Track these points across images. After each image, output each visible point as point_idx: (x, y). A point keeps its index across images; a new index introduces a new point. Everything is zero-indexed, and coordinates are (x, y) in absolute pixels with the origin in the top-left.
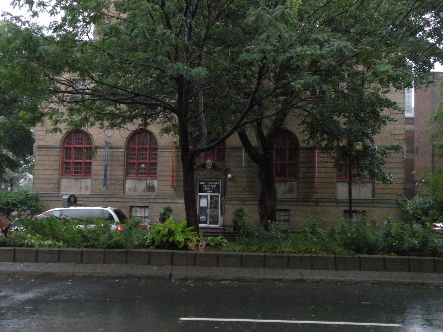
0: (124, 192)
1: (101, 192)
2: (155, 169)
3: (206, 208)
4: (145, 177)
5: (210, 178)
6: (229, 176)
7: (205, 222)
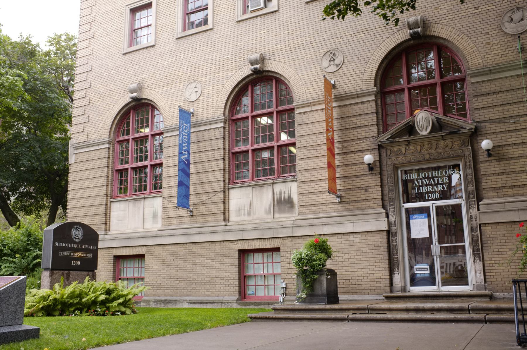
0: (226, 219)
1: (179, 224)
4: (273, 179)
5: (430, 161)
6: (486, 144)
7: (431, 281)
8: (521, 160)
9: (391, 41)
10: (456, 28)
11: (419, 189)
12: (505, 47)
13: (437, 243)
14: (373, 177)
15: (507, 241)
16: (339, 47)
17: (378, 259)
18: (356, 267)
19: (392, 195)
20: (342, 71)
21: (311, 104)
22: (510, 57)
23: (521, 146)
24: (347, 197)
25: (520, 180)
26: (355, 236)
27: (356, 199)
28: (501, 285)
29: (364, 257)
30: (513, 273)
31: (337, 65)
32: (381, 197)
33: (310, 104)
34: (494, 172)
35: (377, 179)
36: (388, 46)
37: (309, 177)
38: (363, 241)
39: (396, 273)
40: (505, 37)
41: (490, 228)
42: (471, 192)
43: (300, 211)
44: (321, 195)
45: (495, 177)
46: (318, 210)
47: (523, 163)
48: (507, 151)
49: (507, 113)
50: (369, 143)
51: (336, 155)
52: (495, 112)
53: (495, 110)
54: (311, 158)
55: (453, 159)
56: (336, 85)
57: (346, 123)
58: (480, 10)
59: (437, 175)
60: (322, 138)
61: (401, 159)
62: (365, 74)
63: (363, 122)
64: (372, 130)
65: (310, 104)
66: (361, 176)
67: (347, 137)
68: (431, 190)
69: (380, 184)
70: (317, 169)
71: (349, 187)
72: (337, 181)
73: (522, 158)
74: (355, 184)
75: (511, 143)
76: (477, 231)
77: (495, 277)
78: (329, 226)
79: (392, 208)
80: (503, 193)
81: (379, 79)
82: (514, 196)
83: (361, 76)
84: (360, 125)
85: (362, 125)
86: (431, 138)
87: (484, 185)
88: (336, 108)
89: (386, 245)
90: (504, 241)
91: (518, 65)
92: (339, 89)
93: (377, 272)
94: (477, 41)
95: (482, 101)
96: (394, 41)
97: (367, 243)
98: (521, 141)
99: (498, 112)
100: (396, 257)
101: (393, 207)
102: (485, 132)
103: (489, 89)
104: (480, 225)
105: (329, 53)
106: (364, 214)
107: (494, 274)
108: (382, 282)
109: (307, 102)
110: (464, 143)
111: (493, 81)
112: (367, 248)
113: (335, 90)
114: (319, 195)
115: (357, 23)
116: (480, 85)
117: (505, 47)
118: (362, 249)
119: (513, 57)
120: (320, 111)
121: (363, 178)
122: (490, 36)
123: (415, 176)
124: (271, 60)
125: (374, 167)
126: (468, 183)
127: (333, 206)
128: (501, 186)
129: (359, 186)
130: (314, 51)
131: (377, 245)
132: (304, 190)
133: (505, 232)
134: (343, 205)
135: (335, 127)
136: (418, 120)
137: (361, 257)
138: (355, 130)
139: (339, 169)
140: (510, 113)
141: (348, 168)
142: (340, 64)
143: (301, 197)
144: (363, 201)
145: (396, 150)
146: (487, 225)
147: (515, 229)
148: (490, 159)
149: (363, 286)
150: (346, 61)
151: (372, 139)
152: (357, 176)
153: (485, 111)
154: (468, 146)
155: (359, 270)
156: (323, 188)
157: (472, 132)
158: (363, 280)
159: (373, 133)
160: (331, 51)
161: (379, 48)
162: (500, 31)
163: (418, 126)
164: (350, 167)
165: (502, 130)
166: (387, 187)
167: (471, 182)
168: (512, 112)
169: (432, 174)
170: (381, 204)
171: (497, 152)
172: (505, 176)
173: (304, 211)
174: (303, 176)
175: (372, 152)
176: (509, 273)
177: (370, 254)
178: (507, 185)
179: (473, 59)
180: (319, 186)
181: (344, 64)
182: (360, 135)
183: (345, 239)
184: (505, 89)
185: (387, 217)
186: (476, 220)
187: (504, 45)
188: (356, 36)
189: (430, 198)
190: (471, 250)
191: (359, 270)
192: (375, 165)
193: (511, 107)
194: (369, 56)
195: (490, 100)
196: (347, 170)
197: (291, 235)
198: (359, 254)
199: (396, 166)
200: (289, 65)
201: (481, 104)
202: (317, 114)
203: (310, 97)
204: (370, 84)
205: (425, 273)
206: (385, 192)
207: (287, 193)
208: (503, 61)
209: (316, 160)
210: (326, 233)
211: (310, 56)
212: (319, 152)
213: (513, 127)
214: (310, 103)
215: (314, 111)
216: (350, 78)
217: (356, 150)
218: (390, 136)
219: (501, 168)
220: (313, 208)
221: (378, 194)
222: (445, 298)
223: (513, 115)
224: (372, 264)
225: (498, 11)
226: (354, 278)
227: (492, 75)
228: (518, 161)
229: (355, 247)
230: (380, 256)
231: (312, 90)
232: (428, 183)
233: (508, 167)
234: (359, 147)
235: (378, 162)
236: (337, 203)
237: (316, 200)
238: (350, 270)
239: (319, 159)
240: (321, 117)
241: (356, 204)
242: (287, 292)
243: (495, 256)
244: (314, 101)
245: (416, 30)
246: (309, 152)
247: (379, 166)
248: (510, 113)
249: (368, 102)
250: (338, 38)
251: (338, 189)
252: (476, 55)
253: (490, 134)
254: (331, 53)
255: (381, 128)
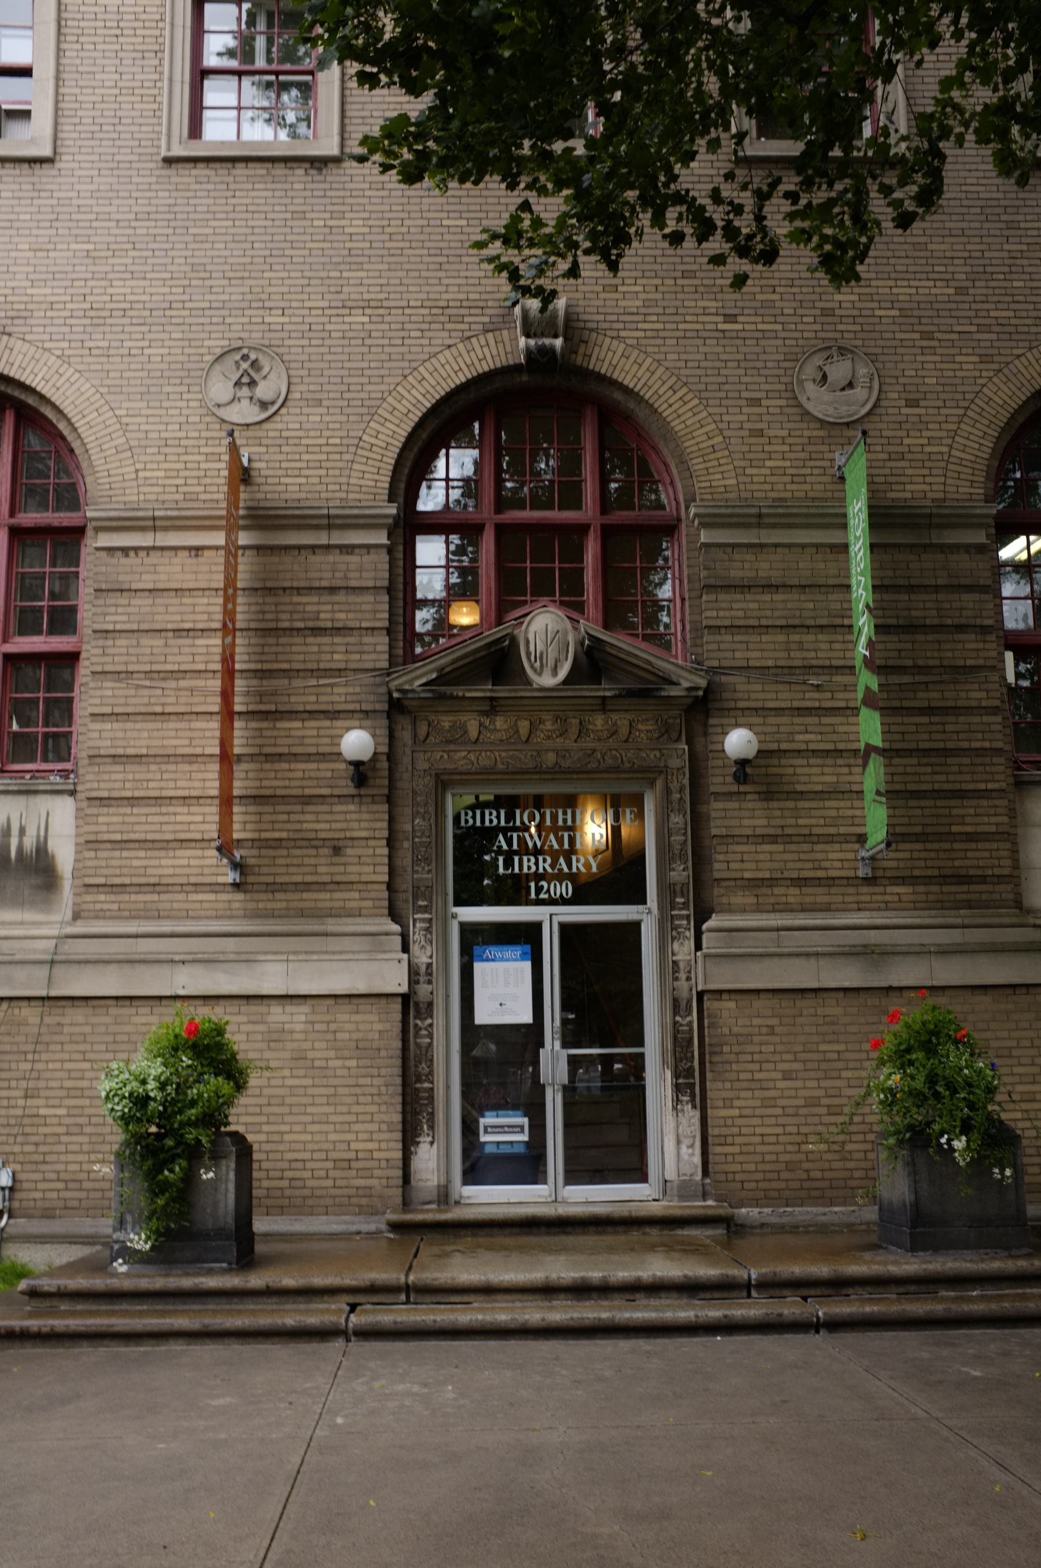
2: (64, 709)
3: (533, 1034)
8: (828, 804)
9: (460, 360)
10: (667, 364)
11: (509, 863)
12: (802, 455)
13: (557, 1045)
14: (364, 808)
15: (779, 1048)
16: (273, 342)
17: (368, 1090)
18: (287, 1119)
19: (424, 875)
20: (279, 426)
21: (153, 524)
22: (815, 487)
23: (829, 761)
24: (264, 870)
25: (824, 864)
26: (290, 1008)
27: (299, 879)
28: (753, 1185)
29: (317, 1081)
30: (790, 1148)
31: (264, 405)
32: (386, 878)
33: (151, 523)
34: (750, 832)
35: (377, 816)
36: (445, 375)
37: (127, 785)
38: (317, 1027)
39: (425, 1140)
40: (805, 425)
41: (732, 1005)
42: (678, 888)
43: (85, 907)
44: (171, 853)
45: (752, 848)
46: (154, 906)
47: (833, 813)
48: (791, 771)
49: (798, 654)
50: (358, 689)
51: (236, 717)
52: (765, 646)
53: (764, 638)
54: (139, 718)
55: (630, 775)
56: (253, 473)
57: (279, 608)
58: (739, 327)
59: (569, 823)
60: (187, 650)
61: (462, 758)
62: (360, 452)
63: (342, 616)
64: (371, 648)
65: (151, 523)
66: (321, 800)
67: (281, 657)
68: (549, 870)
69: (385, 834)
70: (159, 759)
71: (277, 835)
72: (236, 809)
73: (834, 796)
74: (298, 826)
75: (803, 747)
76: (690, 1013)
77: (738, 1158)
78: (198, 970)
79: (423, 920)
80: (772, 900)
81: (404, 478)
82: (804, 909)
83: (346, 457)
84: (329, 625)
85: (337, 625)
86: (566, 702)
87: (719, 868)
88: (247, 552)
89: (399, 1044)
90: (771, 1048)
91: (836, 515)
92: (262, 488)
93: (361, 1136)
94: (725, 418)
95: (728, 606)
96: (469, 362)
97: (330, 1036)
98: (830, 746)
99: (772, 646)
100: (426, 1085)
101: (427, 916)
102: (732, 704)
103: (753, 574)
104: (700, 995)
105: (237, 357)
106: (326, 934)
107: (737, 1149)
108: (377, 1173)
109: (140, 514)
110: (666, 730)
111: (765, 550)
112: (332, 1054)
113: (249, 488)
114: (163, 853)
115: (345, 274)
116: (726, 557)
117: (802, 455)
118: (310, 1055)
119: (822, 487)
120: (186, 553)
121: (325, 808)
122: (764, 410)
123: (498, 817)
124: (10, 335)
125: (369, 774)
126: (672, 860)
127: (211, 897)
128: (768, 876)
129: (313, 835)
130: (180, 336)
131: (367, 1045)
132: (104, 828)
133: (775, 1021)
134: (248, 896)
135: (239, 617)
136: (531, 637)
137: (308, 1082)
138: (310, 640)
139: (244, 766)
140: (805, 654)
141: (276, 766)
142: (273, 403)
143: (92, 854)
144: (322, 887)
145: (447, 725)
146: (725, 996)
147: (805, 1013)
148: (742, 788)
149: (310, 1183)
150: (297, 395)
151: (366, 679)
152: (307, 800)
153: (737, 638)
154: (678, 740)
155: (296, 1128)
156: (178, 827)
157: (697, 697)
158: (309, 1165)
159: (373, 656)
160: (245, 351)
161: (415, 373)
162: (792, 402)
163: (528, 654)
164: (285, 766)
165: (783, 705)
166: (406, 844)
167: (682, 856)
168: (813, 654)
169: (554, 818)
170: (386, 903)
171: (763, 770)
172: (780, 848)
173: (98, 906)
174: (106, 777)
175: (368, 723)
176: (780, 1148)
177: (339, 1072)
178: (786, 874)
179: (711, 471)
180: (166, 819)
181: (289, 403)
182: (328, 657)
183: (253, 1018)
184: (795, 581)
185: (405, 949)
186: (688, 979)
187: (800, 448)
188: (340, 319)
189: (542, 896)
190: (668, 1074)
191: (296, 1128)
192: (374, 769)
193: (811, 637)
194: (380, 395)
195: (752, 605)
196: (273, 775)
197: (43, 993)
198: (302, 1072)
199: (445, 777)
200: (80, 367)
201: (727, 614)
202: (175, 560)
203: (153, 497)
204: (375, 490)
205: (511, 1143)
206: (398, 862)
207: (31, 833)
208: (796, 494)
209: (159, 725)
210: (181, 992)
211: (166, 351)
212: (172, 700)
213: (812, 699)
214: (154, 518)
215: (162, 549)
216: (305, 457)
217: (308, 708)
218: (434, 676)
219: (773, 822)
220: (133, 897)
221: (379, 869)
222: (592, 1229)
223: (815, 662)
224: (344, 1109)
225: (787, 342)
226: (279, 1156)
227: (763, 532)
228: (821, 804)
229: (289, 1045)
230: (376, 1081)
231: (162, 474)
232: (539, 844)
233: (792, 821)
234: (322, 699)
235: (385, 758)
236: (229, 888)
237: (149, 871)
238: (265, 1128)
239: (172, 725)
240: (187, 577)
241: (297, 896)
242: (16, 1204)
243: (743, 1094)
244: (169, 513)
245: (547, 341)
246: (132, 692)
247: (386, 773)
248: (805, 654)
249: (365, 551)
250: (273, 312)
251: (235, 836)
252: (722, 461)
253: (746, 713)
254: (245, 357)
255: (401, 644)
